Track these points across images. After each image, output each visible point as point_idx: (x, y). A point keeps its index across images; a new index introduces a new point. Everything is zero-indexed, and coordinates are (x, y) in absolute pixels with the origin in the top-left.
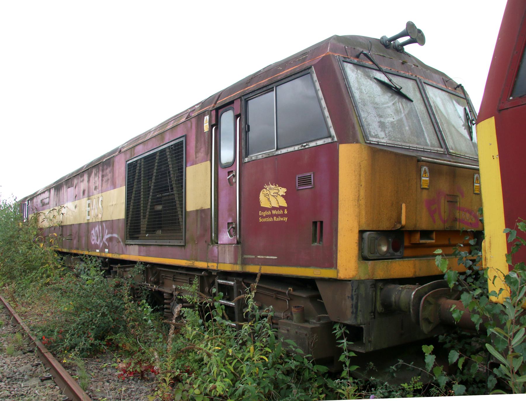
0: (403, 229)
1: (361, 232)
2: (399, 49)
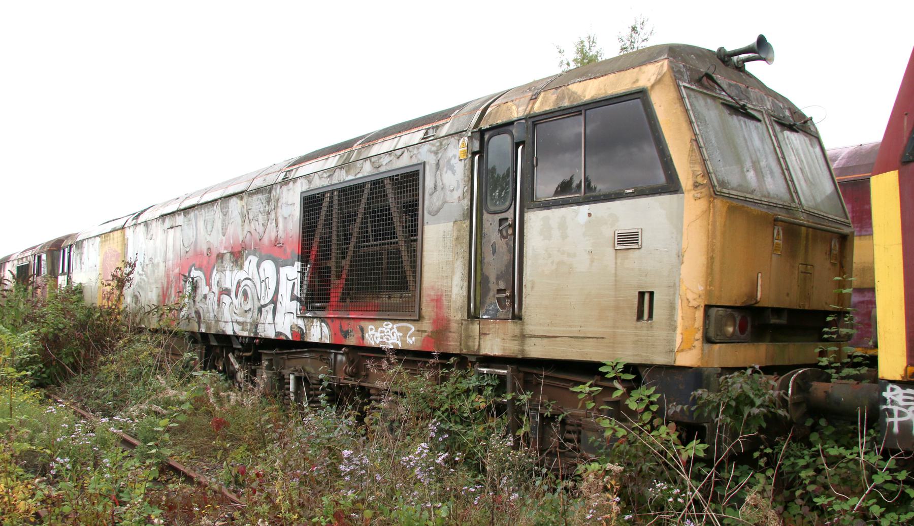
0: (757, 305)
1: (708, 307)
2: (740, 68)
